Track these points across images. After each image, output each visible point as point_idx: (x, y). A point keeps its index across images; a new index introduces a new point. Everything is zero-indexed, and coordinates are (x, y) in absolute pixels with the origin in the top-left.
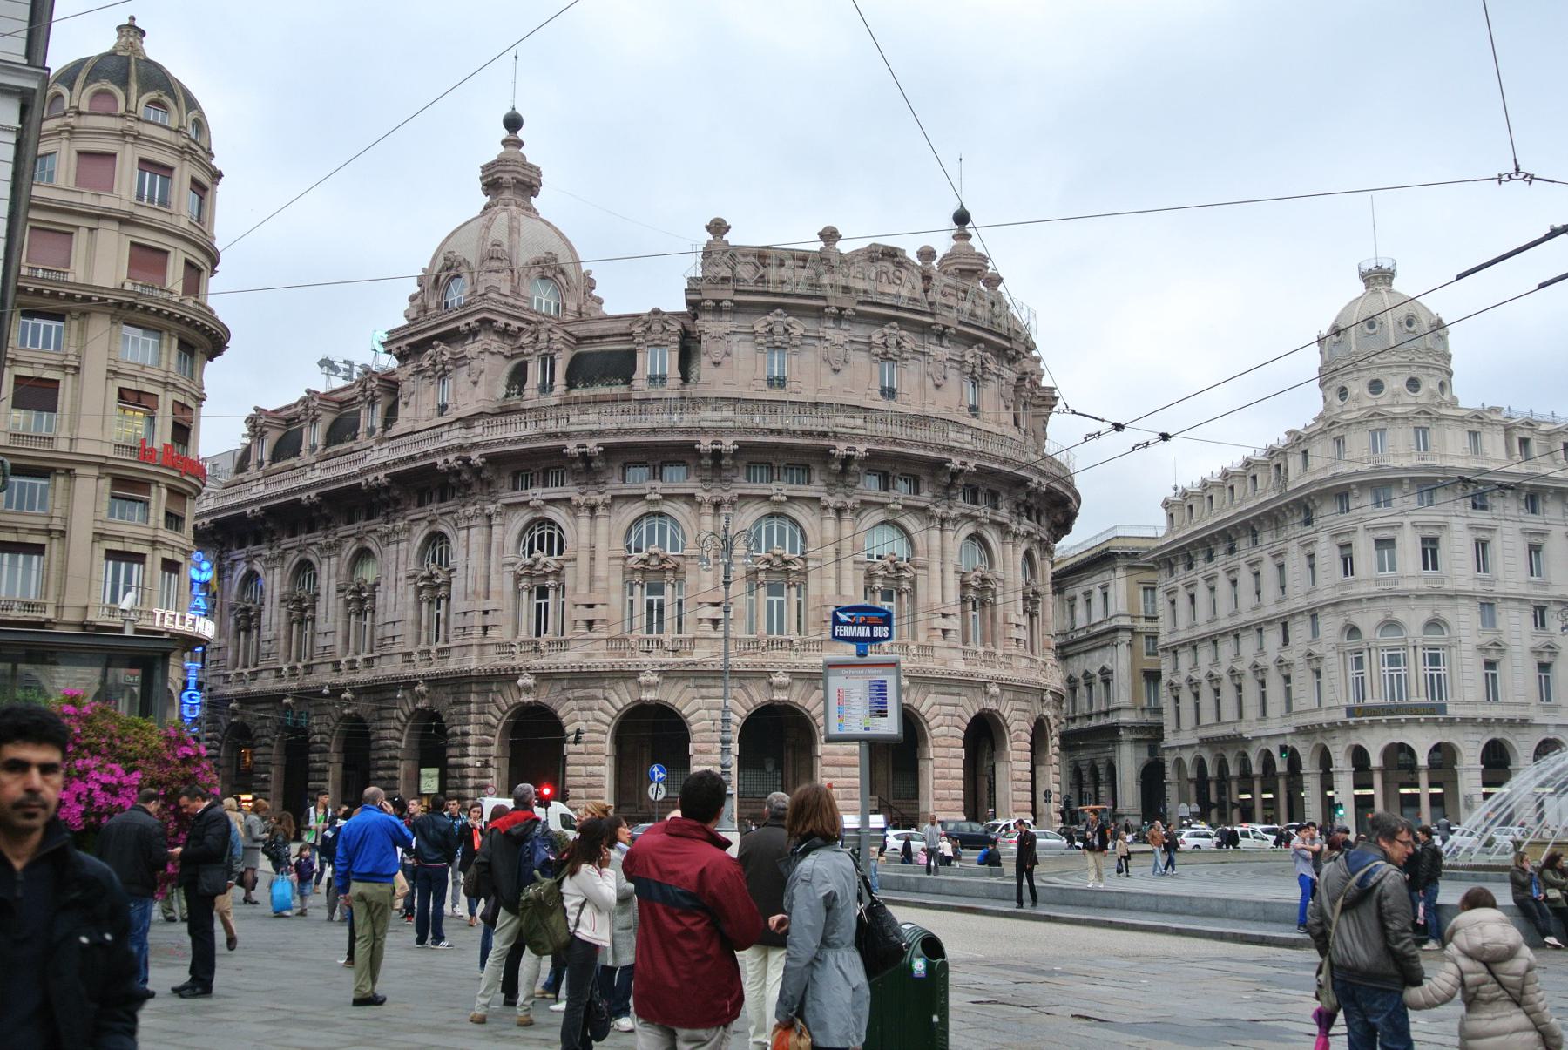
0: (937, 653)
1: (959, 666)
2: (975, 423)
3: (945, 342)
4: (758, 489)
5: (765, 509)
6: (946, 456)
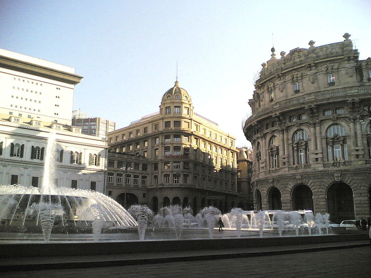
0: (312, 166)
1: (320, 168)
2: (334, 87)
3: (314, 68)
4: (268, 131)
5: (271, 136)
6: (303, 106)
